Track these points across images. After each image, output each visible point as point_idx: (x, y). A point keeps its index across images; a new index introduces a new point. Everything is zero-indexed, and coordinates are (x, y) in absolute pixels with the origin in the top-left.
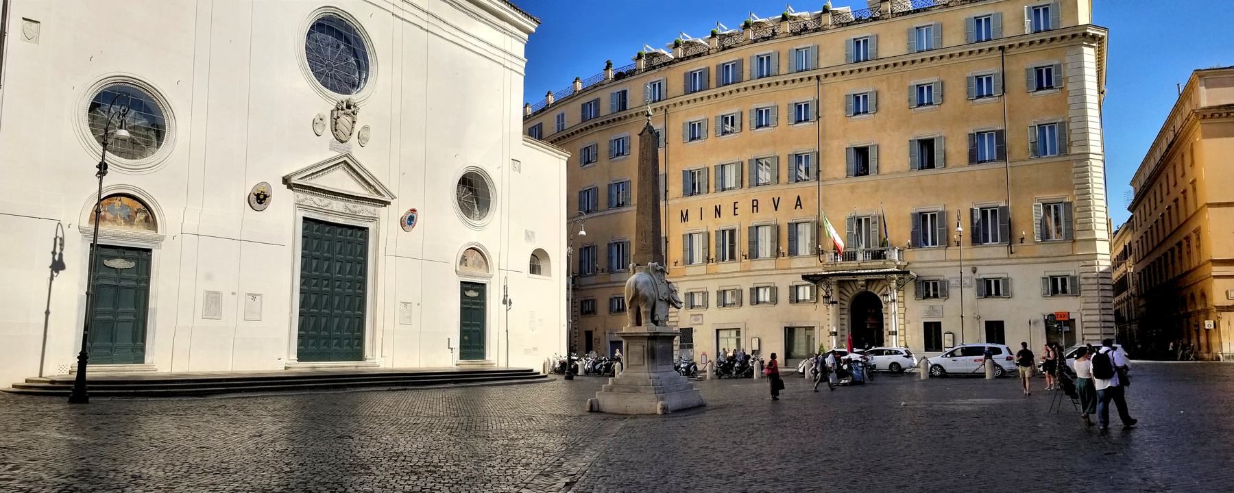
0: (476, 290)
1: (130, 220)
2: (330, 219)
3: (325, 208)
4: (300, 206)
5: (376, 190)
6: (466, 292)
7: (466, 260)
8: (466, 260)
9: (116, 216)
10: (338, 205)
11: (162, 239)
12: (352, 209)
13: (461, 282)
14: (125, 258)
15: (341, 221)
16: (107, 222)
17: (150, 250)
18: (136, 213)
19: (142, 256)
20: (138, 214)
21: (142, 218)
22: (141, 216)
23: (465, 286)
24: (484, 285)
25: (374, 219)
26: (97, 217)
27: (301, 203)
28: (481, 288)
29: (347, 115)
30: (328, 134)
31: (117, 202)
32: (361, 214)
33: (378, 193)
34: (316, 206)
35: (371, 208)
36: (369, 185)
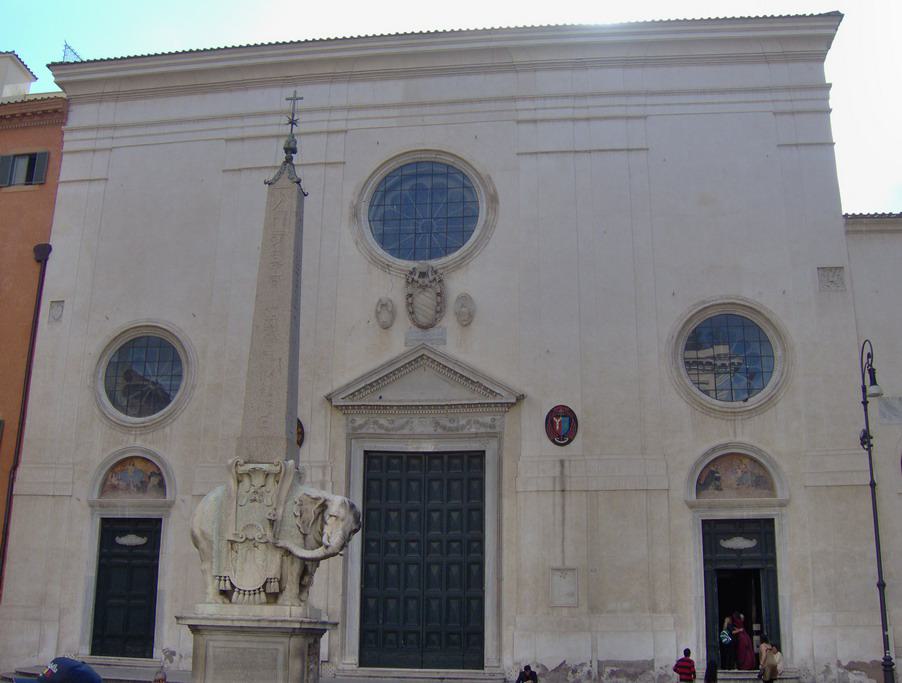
0: (747, 536)
1: (142, 487)
2: (411, 447)
3: (399, 432)
4: (353, 435)
5: (486, 388)
6: (722, 541)
7: (718, 479)
8: (718, 479)
9: (128, 485)
10: (421, 425)
11: (170, 505)
12: (449, 425)
13: (705, 522)
14: (139, 533)
15: (428, 447)
16: (120, 492)
17: (159, 521)
18: (150, 478)
19: (151, 528)
20: (152, 479)
21: (156, 483)
22: (154, 480)
23: (713, 532)
24: (770, 522)
25: (493, 436)
26: (107, 488)
27: (359, 431)
28: (763, 530)
29: (424, 287)
30: (403, 324)
31: (130, 469)
32: (466, 431)
33: (492, 392)
34: (383, 432)
35: (488, 419)
36: (473, 382)
